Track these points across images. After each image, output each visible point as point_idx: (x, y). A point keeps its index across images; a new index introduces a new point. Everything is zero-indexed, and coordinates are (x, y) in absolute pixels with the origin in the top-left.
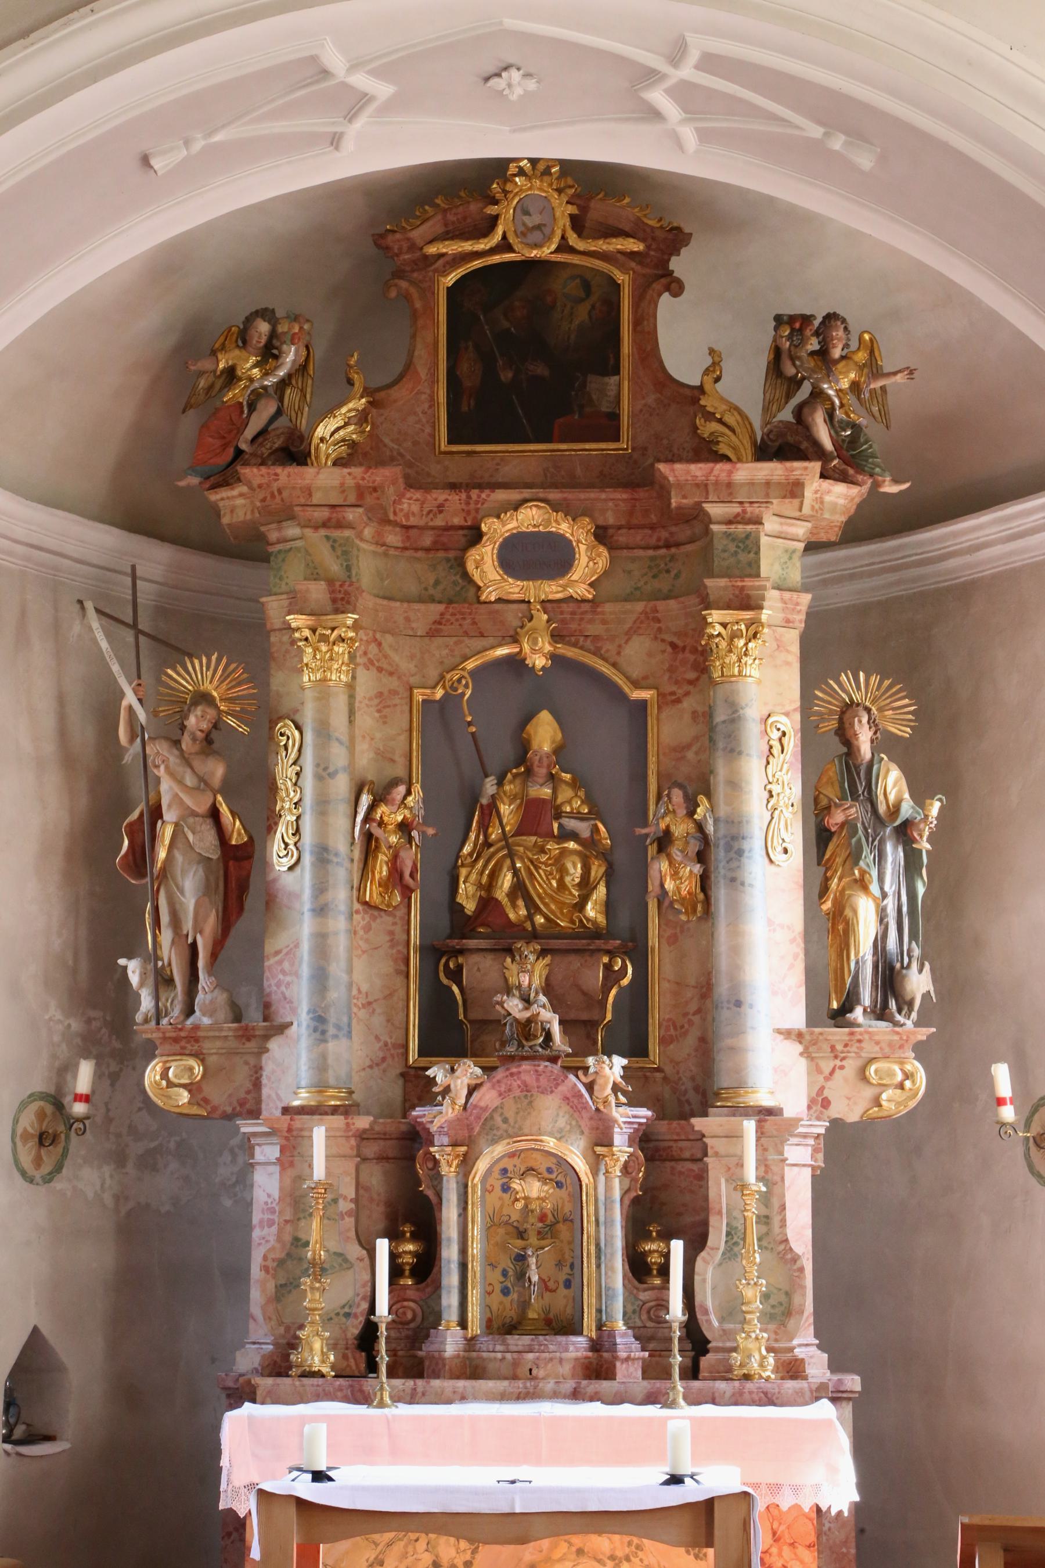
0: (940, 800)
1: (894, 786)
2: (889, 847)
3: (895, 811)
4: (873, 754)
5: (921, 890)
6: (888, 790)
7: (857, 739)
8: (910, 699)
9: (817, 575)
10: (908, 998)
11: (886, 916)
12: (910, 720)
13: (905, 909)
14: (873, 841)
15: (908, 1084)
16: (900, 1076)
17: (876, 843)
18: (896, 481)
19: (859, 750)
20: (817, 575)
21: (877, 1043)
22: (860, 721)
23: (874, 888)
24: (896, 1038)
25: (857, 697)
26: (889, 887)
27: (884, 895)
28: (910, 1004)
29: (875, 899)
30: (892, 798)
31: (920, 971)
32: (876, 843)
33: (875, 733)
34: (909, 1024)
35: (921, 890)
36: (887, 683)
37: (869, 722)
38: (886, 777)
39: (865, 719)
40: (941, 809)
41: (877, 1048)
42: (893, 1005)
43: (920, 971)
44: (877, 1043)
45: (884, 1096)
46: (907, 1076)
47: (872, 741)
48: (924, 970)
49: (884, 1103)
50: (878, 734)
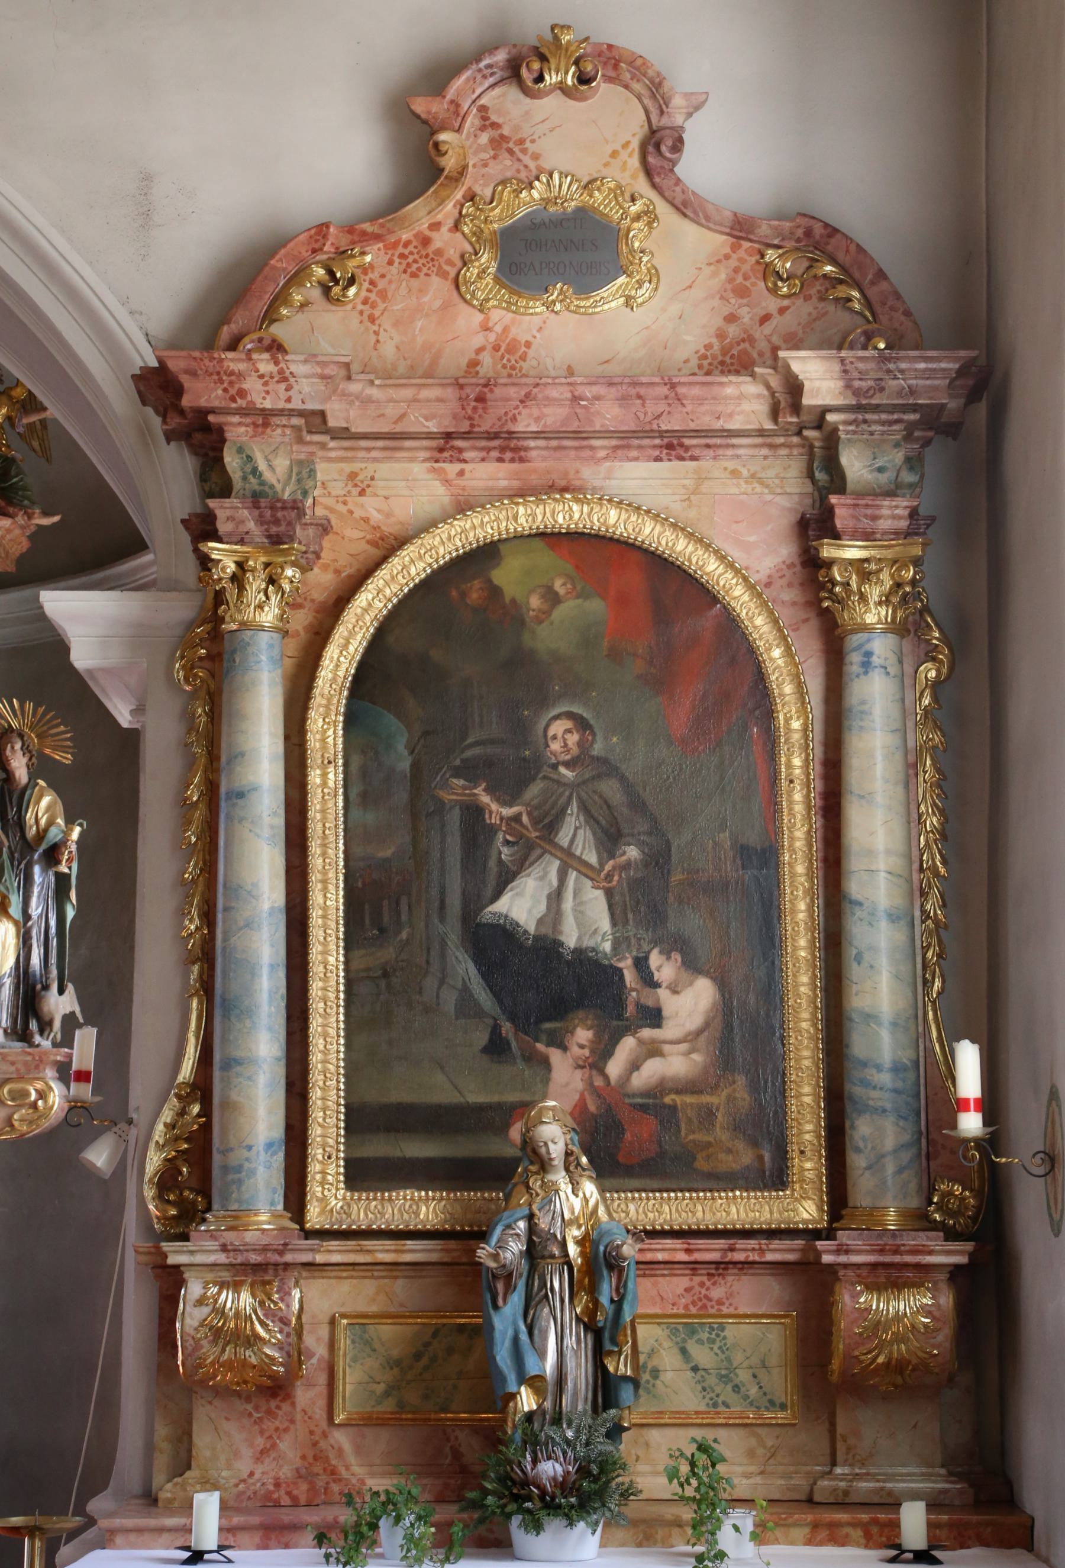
0: (81, 825)
1: (46, 811)
2: (37, 869)
3: (41, 835)
4: (30, 779)
5: (70, 913)
6: (40, 815)
7: (9, 765)
8: (66, 726)
9: (31, 610)
10: (47, 1019)
11: (31, 938)
12: (69, 747)
13: (53, 930)
14: (19, 864)
15: (40, 1103)
16: (33, 1096)
17: (22, 866)
18: (46, 514)
19: (14, 775)
20: (31, 610)
21: (13, 1063)
22: (13, 748)
23: (15, 910)
24: (29, 1058)
25: (15, 724)
26: (36, 909)
27: (27, 916)
28: (50, 1023)
29: (16, 923)
30: (43, 822)
31: (61, 991)
32: (22, 866)
33: (30, 759)
34: (46, 1044)
35: (70, 913)
36: (41, 710)
37: (22, 749)
38: (38, 802)
39: (18, 746)
40: (81, 834)
41: (13, 1069)
42: (34, 1025)
43: (61, 991)
44: (13, 1063)
45: (16, 1117)
46: (41, 1095)
47: (28, 766)
48: (67, 992)
49: (16, 1124)
50: (34, 760)
